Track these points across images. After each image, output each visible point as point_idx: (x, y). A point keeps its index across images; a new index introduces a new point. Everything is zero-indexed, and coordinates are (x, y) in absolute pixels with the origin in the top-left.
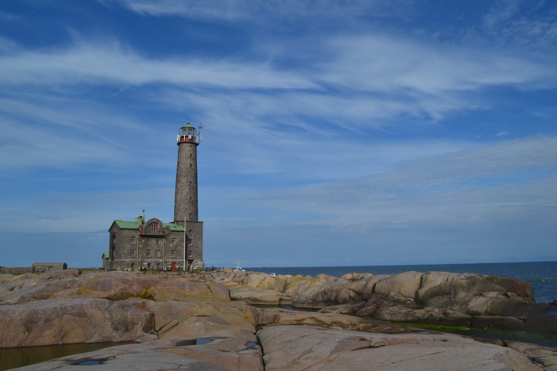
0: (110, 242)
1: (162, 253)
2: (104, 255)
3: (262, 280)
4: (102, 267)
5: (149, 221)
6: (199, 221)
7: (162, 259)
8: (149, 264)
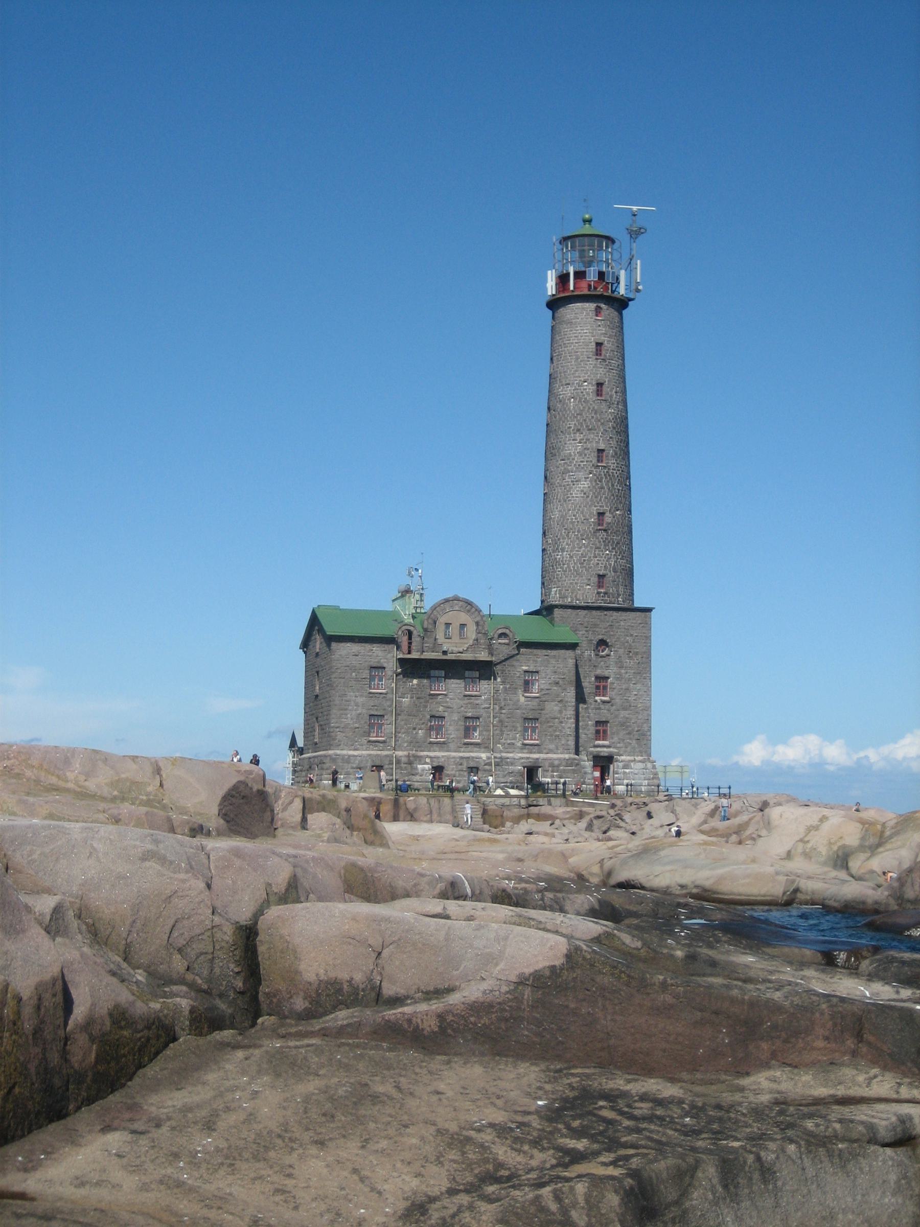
3: (810, 829)
8: (438, 770)
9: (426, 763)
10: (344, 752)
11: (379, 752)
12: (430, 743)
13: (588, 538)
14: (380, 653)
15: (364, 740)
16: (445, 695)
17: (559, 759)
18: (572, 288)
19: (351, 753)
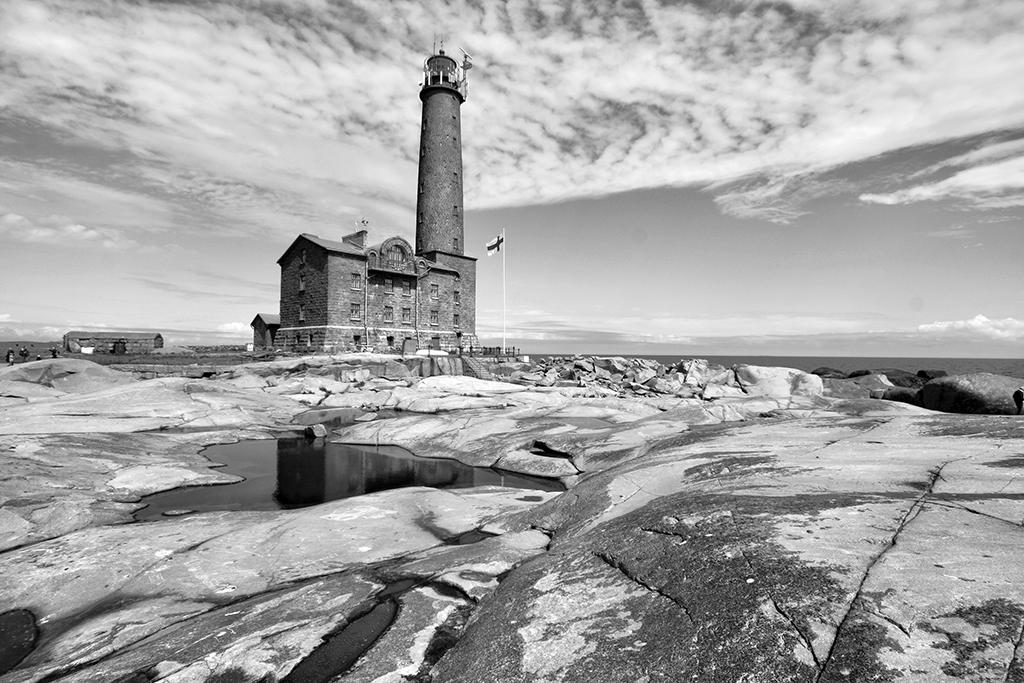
6: (465, 255)
8: (390, 339)
14: (358, 266)
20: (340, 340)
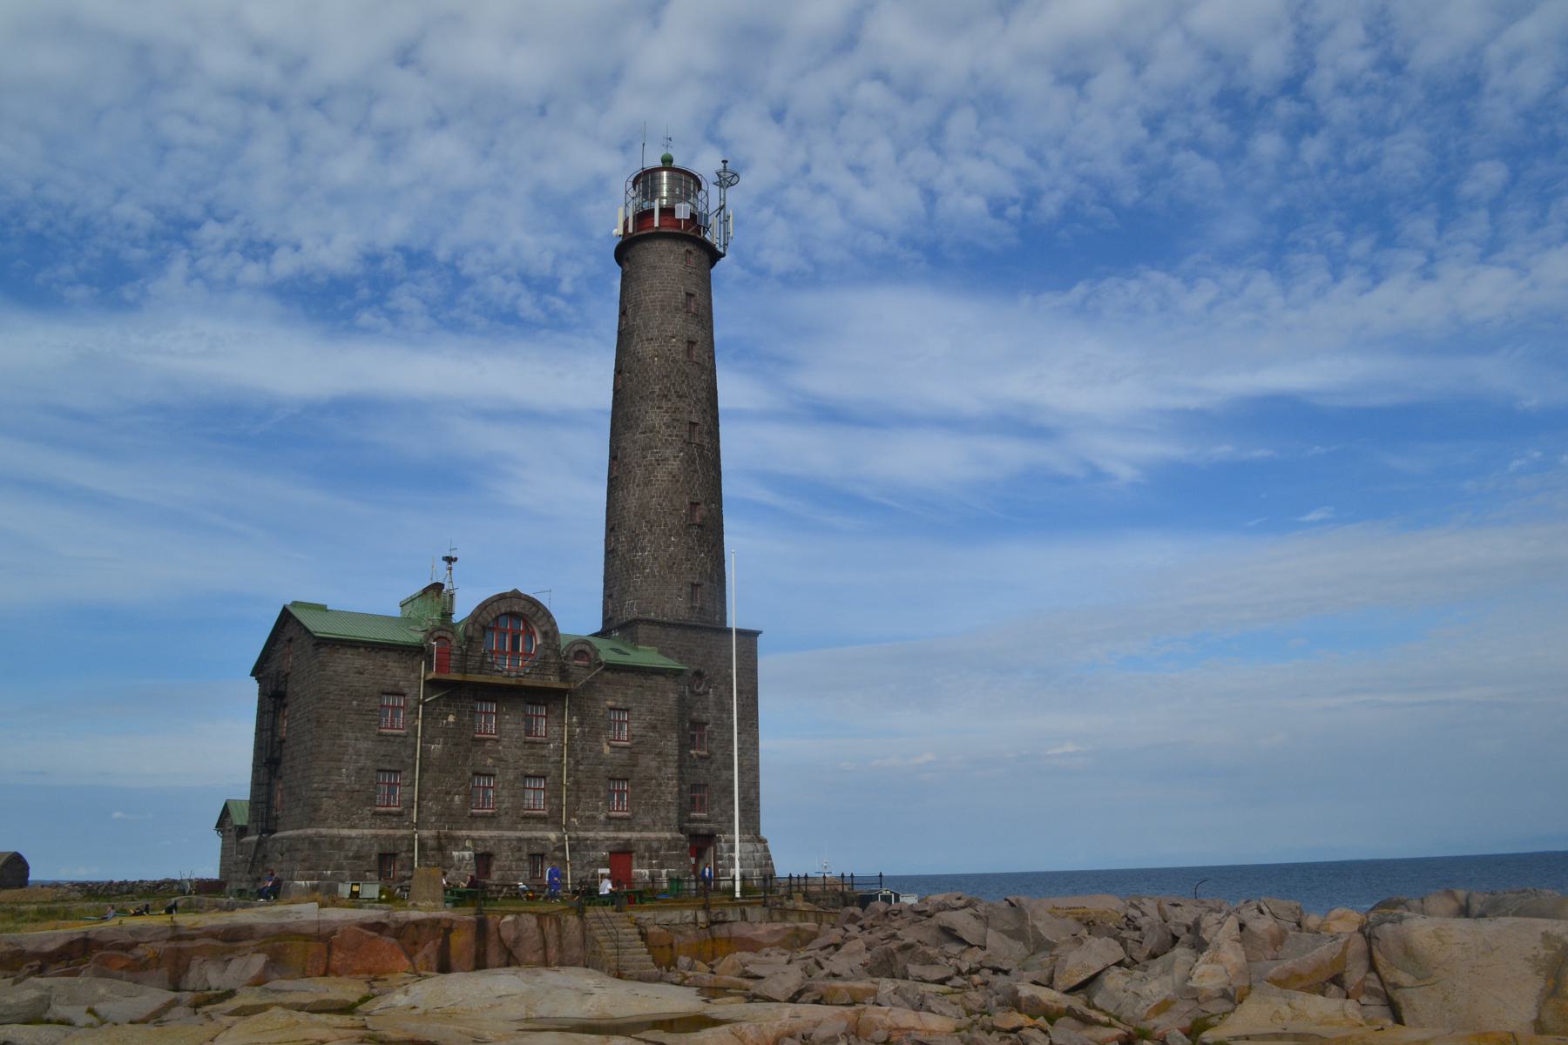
0: (260, 730)
1: (554, 792)
2: (226, 812)
4: (212, 871)
5: (484, 607)
7: (558, 825)
8: (484, 860)
9: (465, 849)
10: (335, 831)
11: (391, 832)
12: (472, 815)
13: (678, 534)
14: (399, 672)
15: (367, 811)
16: (498, 741)
17: (659, 840)
18: (656, 224)
19: (345, 832)
20: (339, 867)
